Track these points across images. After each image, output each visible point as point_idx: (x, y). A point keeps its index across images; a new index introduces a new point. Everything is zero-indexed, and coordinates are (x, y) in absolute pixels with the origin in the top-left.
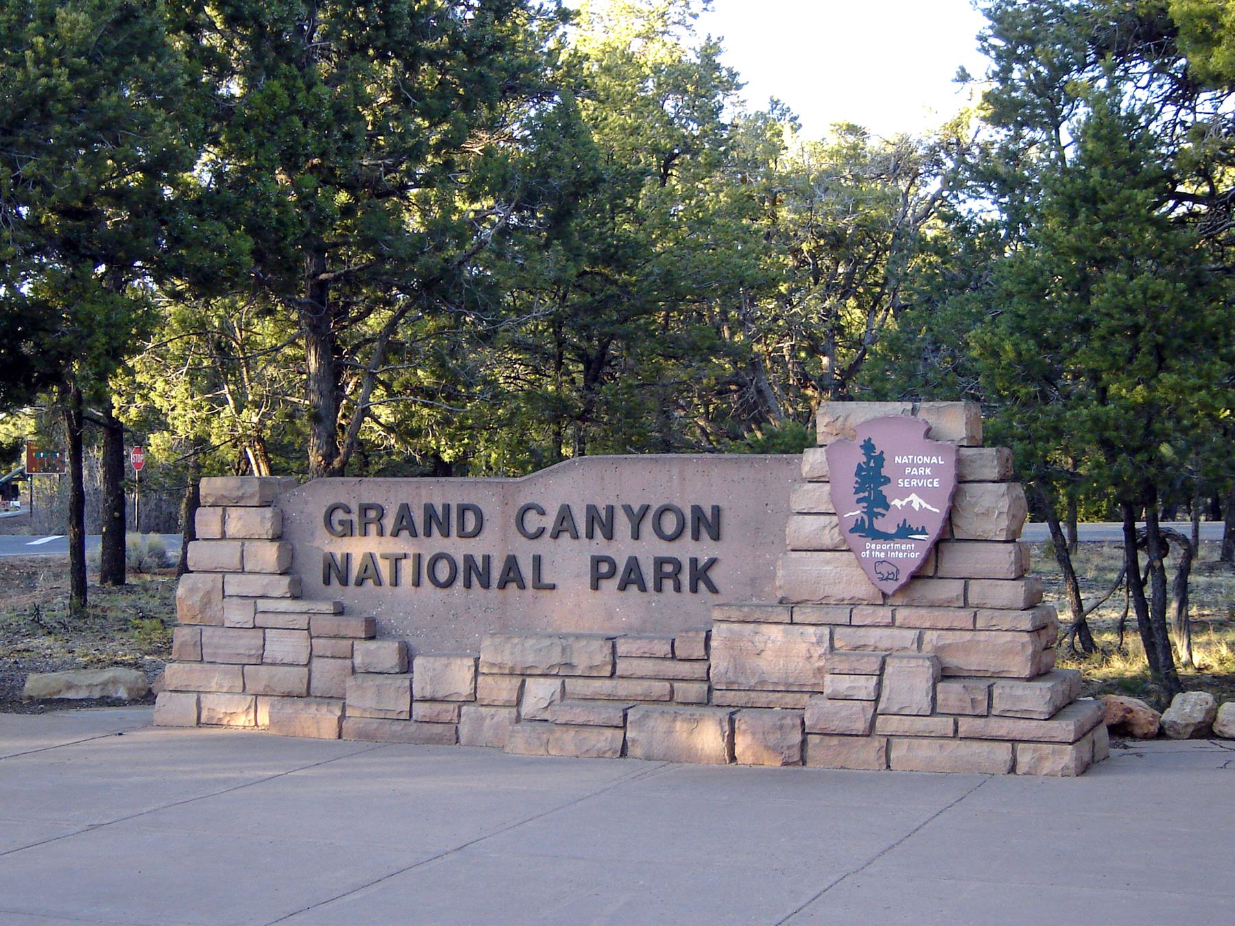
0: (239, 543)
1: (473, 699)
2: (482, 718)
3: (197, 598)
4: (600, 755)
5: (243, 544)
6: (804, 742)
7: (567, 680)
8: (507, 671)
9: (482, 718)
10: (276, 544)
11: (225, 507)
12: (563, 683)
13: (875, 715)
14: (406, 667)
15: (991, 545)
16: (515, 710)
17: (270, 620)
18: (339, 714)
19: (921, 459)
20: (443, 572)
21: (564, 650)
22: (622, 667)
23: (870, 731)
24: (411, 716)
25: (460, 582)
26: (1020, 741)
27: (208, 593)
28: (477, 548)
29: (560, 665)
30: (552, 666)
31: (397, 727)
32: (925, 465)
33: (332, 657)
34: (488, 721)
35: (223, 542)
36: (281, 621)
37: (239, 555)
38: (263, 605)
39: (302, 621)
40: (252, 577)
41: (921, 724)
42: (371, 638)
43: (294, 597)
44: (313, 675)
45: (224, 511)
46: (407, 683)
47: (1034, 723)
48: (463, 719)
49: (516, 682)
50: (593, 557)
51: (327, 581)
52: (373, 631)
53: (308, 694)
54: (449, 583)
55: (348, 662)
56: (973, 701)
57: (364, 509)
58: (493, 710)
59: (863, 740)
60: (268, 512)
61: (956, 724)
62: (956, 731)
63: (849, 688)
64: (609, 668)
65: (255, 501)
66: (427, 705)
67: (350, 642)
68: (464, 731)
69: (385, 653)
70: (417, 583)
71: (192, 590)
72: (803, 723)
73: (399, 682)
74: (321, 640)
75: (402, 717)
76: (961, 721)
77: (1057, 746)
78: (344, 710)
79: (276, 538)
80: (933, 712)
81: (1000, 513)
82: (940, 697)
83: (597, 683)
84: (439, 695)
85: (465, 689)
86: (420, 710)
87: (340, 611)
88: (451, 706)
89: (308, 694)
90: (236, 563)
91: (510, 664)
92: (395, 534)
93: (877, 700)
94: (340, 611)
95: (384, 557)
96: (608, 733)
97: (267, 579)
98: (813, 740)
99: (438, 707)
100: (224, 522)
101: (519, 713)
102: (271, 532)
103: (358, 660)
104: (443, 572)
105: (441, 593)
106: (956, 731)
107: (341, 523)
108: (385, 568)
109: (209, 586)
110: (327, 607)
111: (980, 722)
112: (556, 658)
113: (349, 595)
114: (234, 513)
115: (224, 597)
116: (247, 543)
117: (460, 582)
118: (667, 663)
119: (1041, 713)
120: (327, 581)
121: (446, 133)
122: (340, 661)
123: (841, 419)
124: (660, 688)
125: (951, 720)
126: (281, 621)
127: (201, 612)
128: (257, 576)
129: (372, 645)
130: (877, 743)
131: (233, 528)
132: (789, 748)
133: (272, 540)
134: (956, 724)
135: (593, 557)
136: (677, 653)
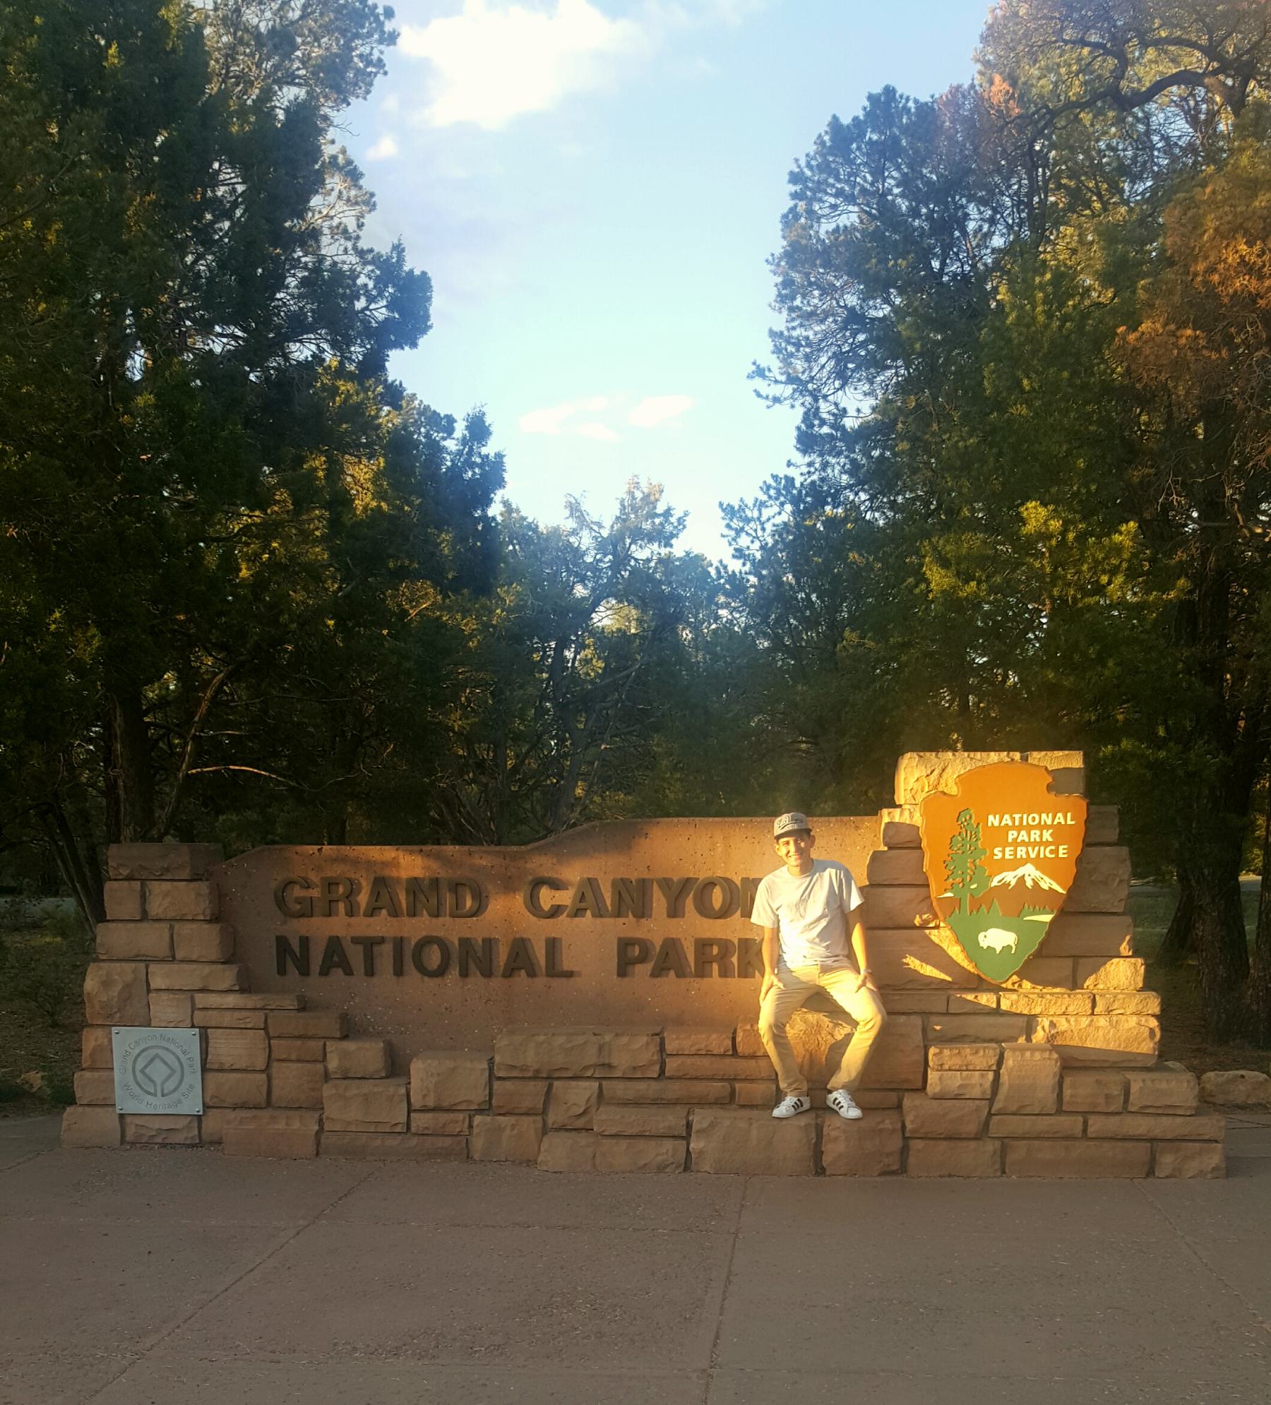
0: (165, 926)
1: (486, 1108)
2: (500, 1129)
3: (115, 991)
4: (661, 1168)
5: (172, 928)
6: (904, 1151)
7: (604, 1083)
8: (530, 1074)
9: (500, 1129)
10: (217, 927)
11: (143, 881)
12: (600, 1087)
13: (990, 1114)
14: (396, 1067)
15: (1105, 918)
16: (539, 1118)
17: (214, 1018)
18: (317, 1128)
19: (1032, 819)
20: (433, 957)
21: (601, 1048)
22: (672, 1065)
23: (983, 1132)
24: (408, 1128)
25: (454, 973)
26: (1161, 1140)
27: (127, 986)
28: (475, 929)
29: (596, 1066)
30: (586, 1068)
31: (393, 1142)
32: (1041, 827)
33: (298, 1061)
34: (508, 1132)
35: (145, 925)
36: (228, 1019)
37: (168, 939)
38: (201, 999)
39: (258, 1019)
40: (186, 966)
41: (1043, 1124)
42: (345, 1037)
43: (242, 991)
44: (275, 1082)
45: (142, 886)
46: (403, 1091)
47: (1179, 1120)
48: (476, 1131)
49: (541, 1086)
50: (620, 940)
51: (282, 971)
52: (349, 1029)
53: (269, 1104)
54: (441, 972)
55: (320, 1067)
56: (1107, 1097)
57: (331, 884)
58: (512, 1119)
59: (973, 1144)
60: (203, 887)
61: (1085, 1123)
62: (1085, 1130)
63: (960, 1086)
64: (657, 1068)
65: (185, 874)
66: (430, 1115)
67: (322, 1043)
68: (478, 1143)
69: (369, 1054)
70: (399, 972)
71: (106, 983)
72: (904, 1126)
73: (392, 1090)
74: (282, 1042)
75: (398, 1129)
76: (1092, 1120)
77: (1205, 1145)
78: (321, 1122)
79: (215, 919)
80: (1060, 1111)
81: (1121, 881)
82: (1067, 1092)
83: (642, 1086)
84: (446, 1104)
85: (480, 1095)
86: (420, 1121)
87: (304, 1006)
88: (461, 1116)
89: (269, 1104)
90: (163, 950)
91: (536, 1067)
92: (372, 911)
93: (991, 1101)
94: (304, 1006)
95: (355, 940)
96: (668, 1145)
97: (207, 969)
98: (916, 1145)
99: (444, 1117)
100: (143, 898)
101: (544, 1121)
102: (208, 912)
103: (333, 1063)
104: (433, 957)
105: (431, 983)
106: (1085, 1130)
107: (299, 901)
108: (356, 956)
109: (129, 978)
110: (289, 1002)
111: (1114, 1120)
112: (591, 1057)
113: (316, 986)
114: (157, 888)
115: (149, 991)
116: (177, 926)
117: (454, 973)
118: (727, 1061)
119: (1189, 1108)
120: (282, 971)
121: (985, 390)
122: (309, 1066)
123: (936, 773)
124: (718, 1088)
125: (1081, 1119)
126: (228, 1019)
127: (119, 1010)
128: (194, 966)
129: (350, 1046)
130: (991, 1146)
131: (156, 907)
132: (888, 1155)
133: (210, 921)
134: (1085, 1123)
135: (620, 940)
136: (740, 1050)
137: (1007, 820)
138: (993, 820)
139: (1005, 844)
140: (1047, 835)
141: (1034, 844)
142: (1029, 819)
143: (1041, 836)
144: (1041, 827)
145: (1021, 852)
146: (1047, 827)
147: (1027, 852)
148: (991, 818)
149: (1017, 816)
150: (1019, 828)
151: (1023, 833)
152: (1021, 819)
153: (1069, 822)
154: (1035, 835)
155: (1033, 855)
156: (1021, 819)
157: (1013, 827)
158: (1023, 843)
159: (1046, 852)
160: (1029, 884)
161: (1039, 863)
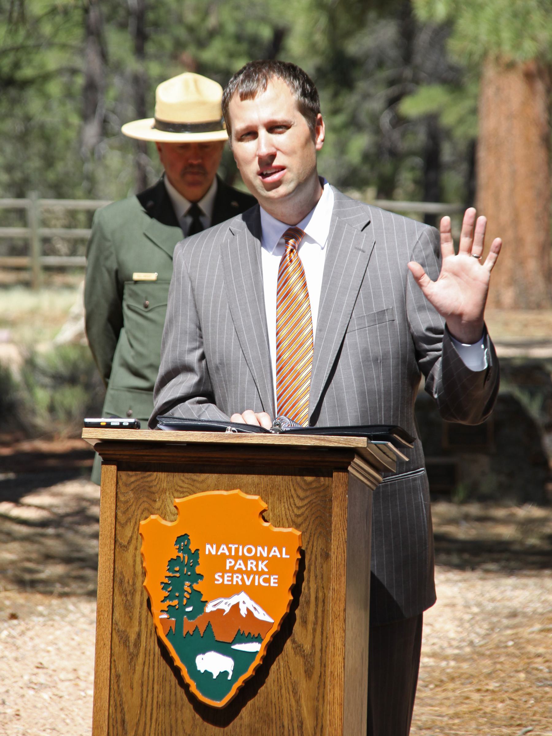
137: (223, 549)
138: (211, 549)
139: (224, 571)
140: (262, 566)
141: (248, 573)
142: (243, 551)
143: (257, 566)
144: (255, 558)
145: (237, 579)
146: (262, 558)
147: (243, 580)
148: (208, 547)
149: (233, 547)
150: (236, 558)
151: (240, 562)
152: (237, 550)
153: (284, 556)
154: (251, 565)
155: (248, 583)
156: (237, 550)
157: (230, 557)
158: (240, 571)
159: (260, 581)
160: (243, 612)
161: (254, 592)
